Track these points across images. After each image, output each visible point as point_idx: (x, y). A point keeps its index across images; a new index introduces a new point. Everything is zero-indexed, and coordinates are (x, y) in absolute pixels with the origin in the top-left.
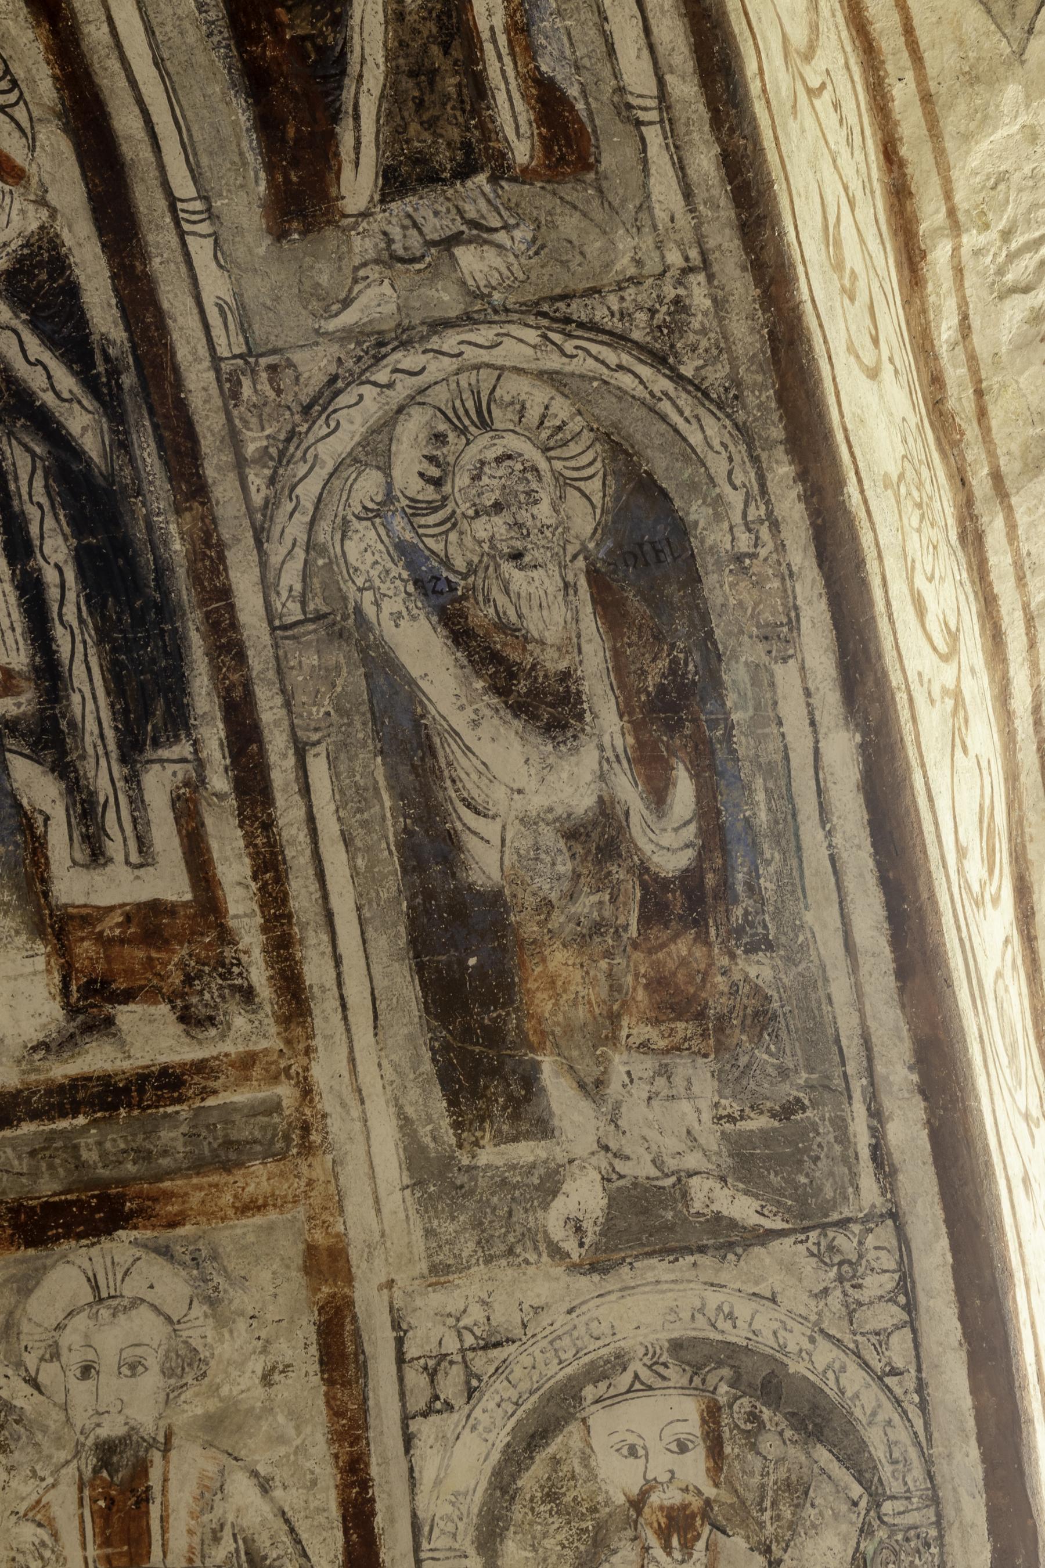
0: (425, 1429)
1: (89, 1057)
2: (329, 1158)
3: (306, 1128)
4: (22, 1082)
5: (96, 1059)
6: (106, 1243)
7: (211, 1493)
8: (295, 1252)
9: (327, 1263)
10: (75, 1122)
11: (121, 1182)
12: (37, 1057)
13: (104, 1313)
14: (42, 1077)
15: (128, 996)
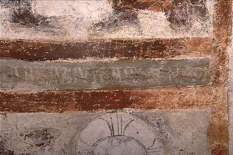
1: (123, 32)
2: (226, 88)
3: (218, 74)
4: (89, 39)
5: (126, 33)
6: (119, 113)
8: (203, 125)
10: (112, 59)
11: (131, 88)
12: (98, 29)
13: (115, 141)
14: (99, 38)
15: (145, 6)
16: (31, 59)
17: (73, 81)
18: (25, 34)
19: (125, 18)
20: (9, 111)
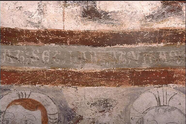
1: (169, 22)
4: (141, 29)
6: (165, 87)
10: (159, 45)
11: (175, 68)
12: (148, 20)
13: (161, 110)
14: (149, 28)
16: (95, 45)
17: (127, 62)
18: (91, 26)
19: (172, 11)
20: (79, 85)
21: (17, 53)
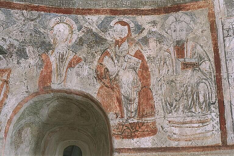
0: (227, 39)
7: (194, 48)
9: (212, 16)
11: (181, 4)
17: (162, 4)
20: (142, 15)
21: (117, 3)
